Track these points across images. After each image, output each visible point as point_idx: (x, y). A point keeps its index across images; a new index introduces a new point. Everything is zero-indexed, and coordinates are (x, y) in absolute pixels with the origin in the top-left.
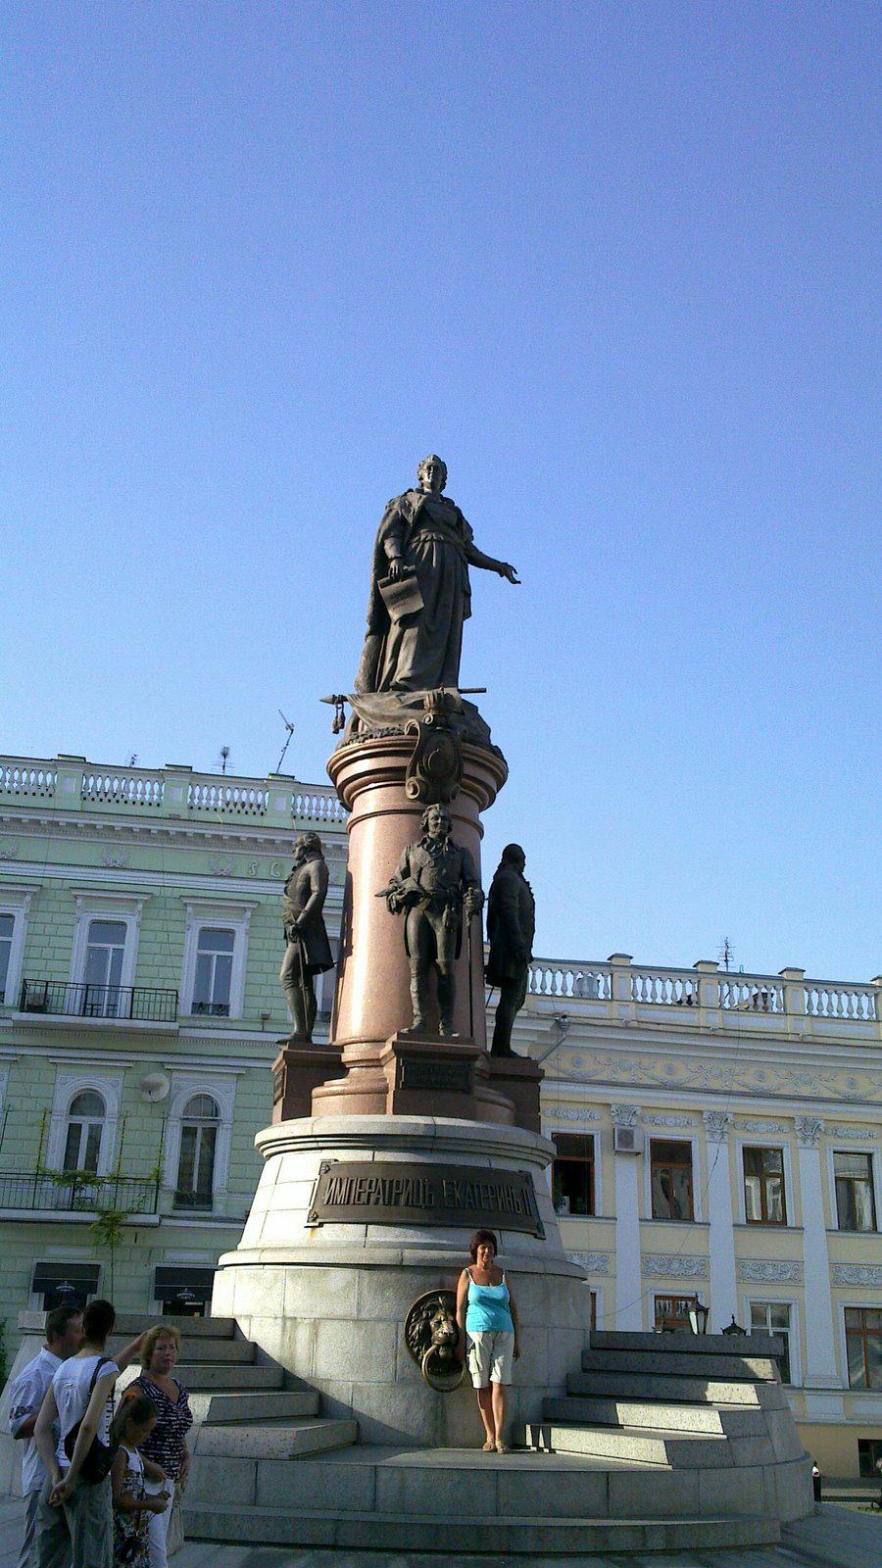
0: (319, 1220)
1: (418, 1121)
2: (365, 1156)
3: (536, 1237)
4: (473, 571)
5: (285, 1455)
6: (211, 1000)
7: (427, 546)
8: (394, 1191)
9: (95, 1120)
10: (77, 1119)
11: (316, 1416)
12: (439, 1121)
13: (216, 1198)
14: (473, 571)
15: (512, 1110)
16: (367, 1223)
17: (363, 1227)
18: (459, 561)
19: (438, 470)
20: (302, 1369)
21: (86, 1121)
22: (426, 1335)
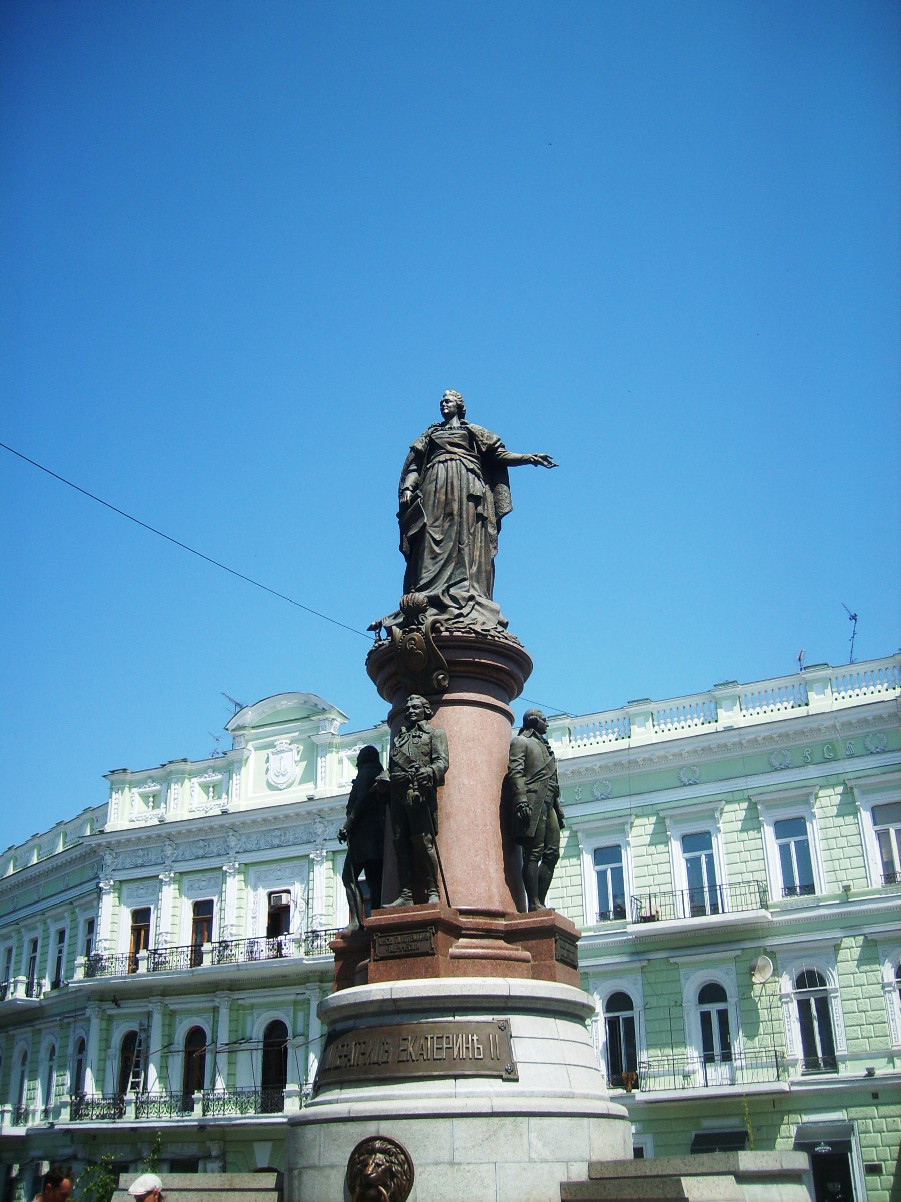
3: (504, 1080)
4: (509, 468)
6: (797, 883)
9: (721, 1006)
10: (706, 1007)
14: (509, 468)
18: (464, 471)
21: (713, 1008)
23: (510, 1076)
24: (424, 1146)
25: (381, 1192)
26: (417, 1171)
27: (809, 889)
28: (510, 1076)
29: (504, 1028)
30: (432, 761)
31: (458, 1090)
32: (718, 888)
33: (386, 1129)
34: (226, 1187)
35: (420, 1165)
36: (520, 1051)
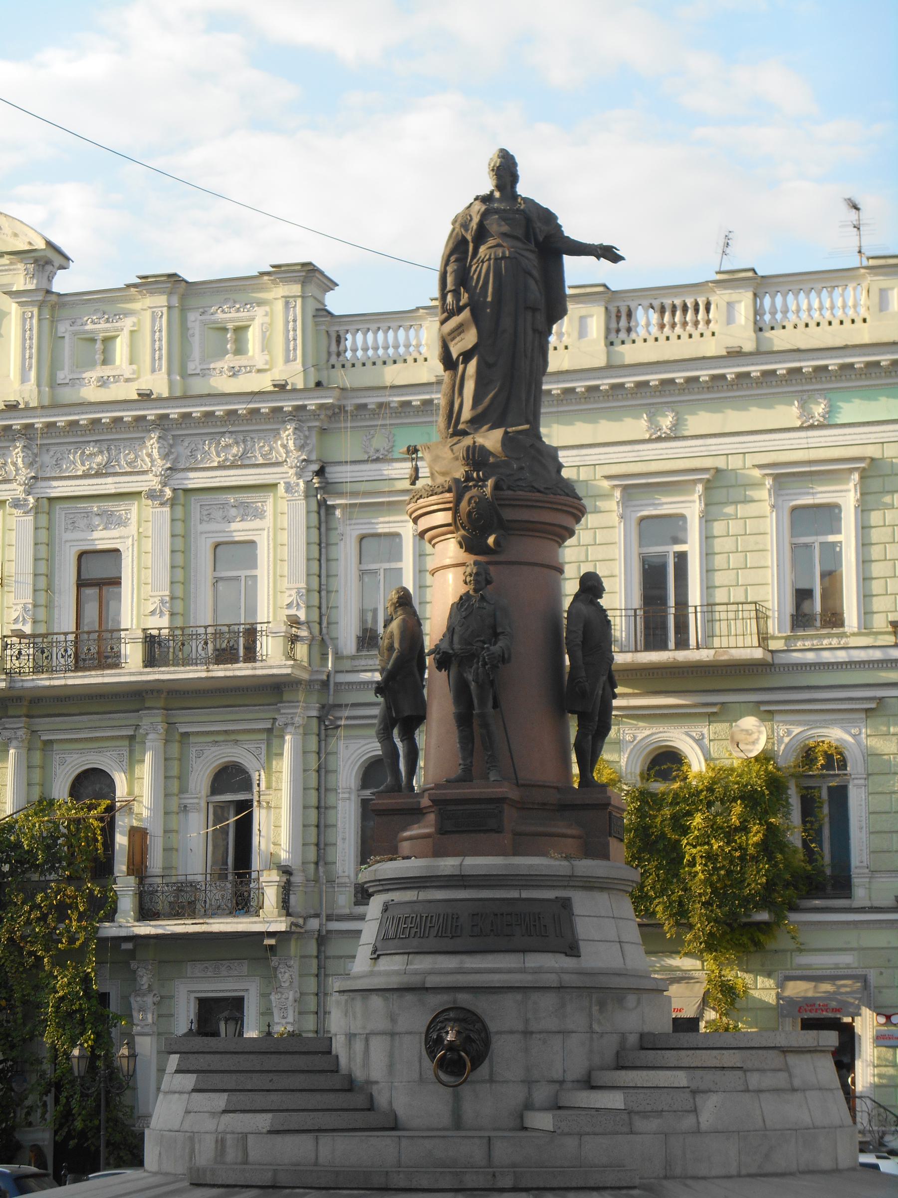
0: (378, 953)
1: (448, 865)
2: (409, 896)
4: (567, 260)
5: (265, 1130)
7: (485, 265)
8: (428, 925)
11: (369, 1110)
12: (470, 861)
13: (855, 881)
14: (567, 260)
15: (579, 837)
16: (409, 953)
17: (406, 957)
19: (506, 170)
20: (359, 1074)
22: (440, 1040)
23: (572, 950)
24: (502, 1017)
25: (461, 1056)
26: (494, 1039)
27: (833, 619)
28: (572, 950)
29: (566, 904)
30: (495, 635)
31: (527, 965)
32: (691, 610)
33: (464, 999)
34: (272, 1050)
35: (497, 1033)
36: (584, 928)
